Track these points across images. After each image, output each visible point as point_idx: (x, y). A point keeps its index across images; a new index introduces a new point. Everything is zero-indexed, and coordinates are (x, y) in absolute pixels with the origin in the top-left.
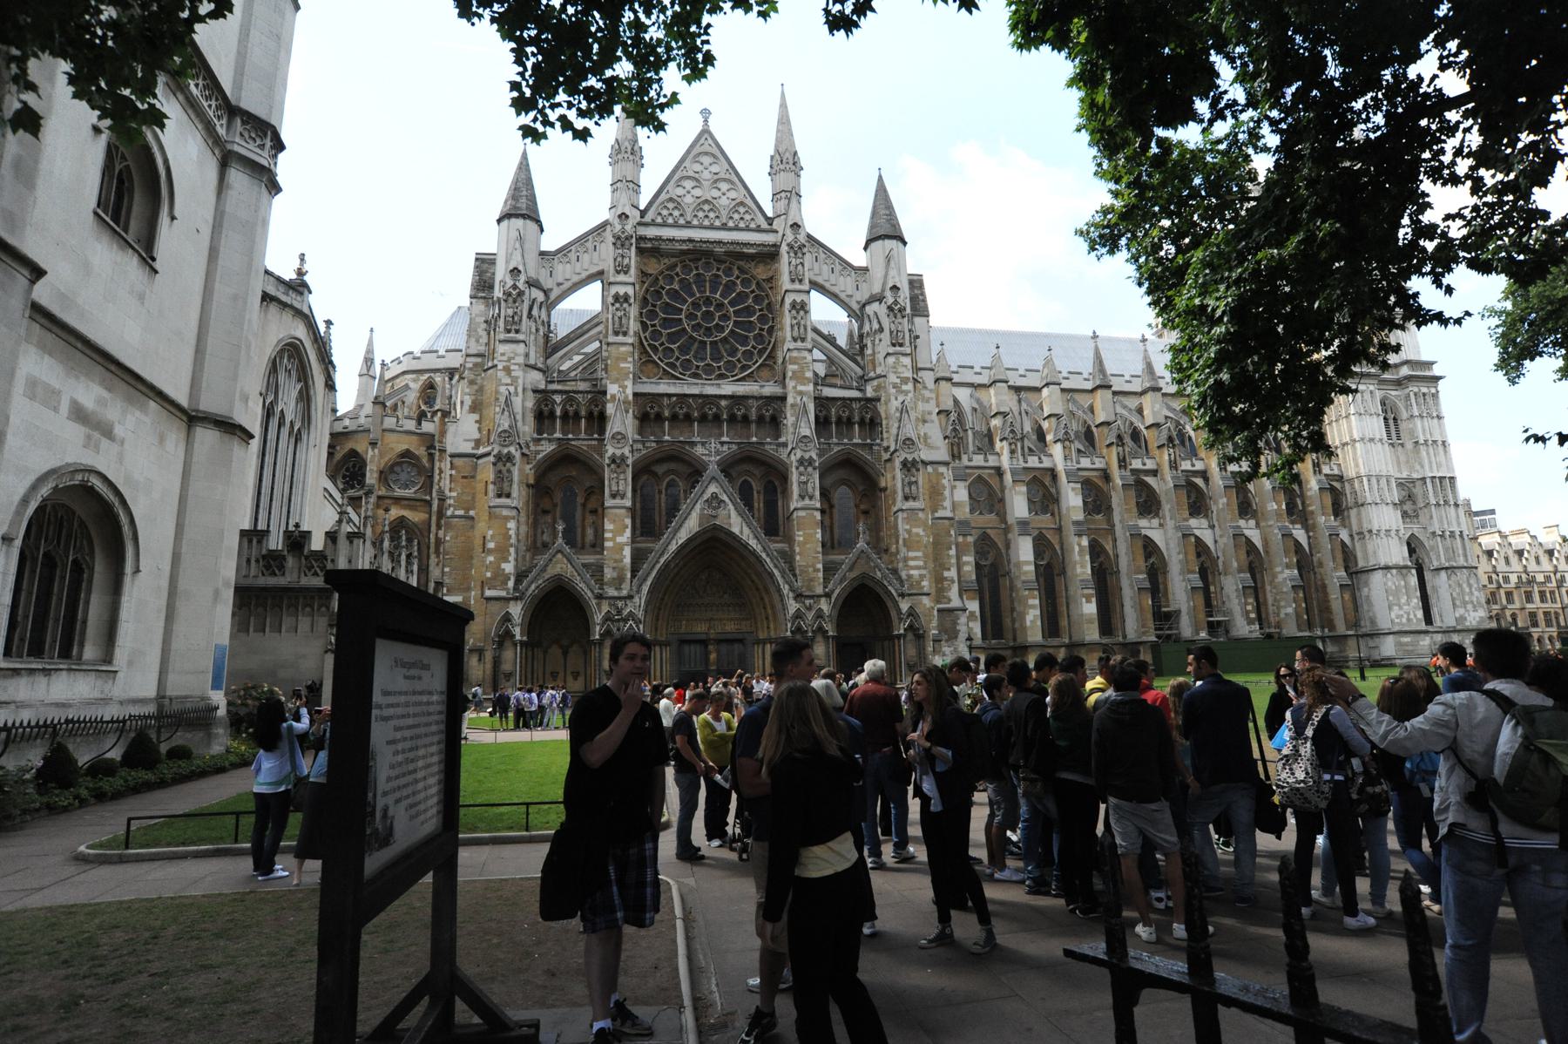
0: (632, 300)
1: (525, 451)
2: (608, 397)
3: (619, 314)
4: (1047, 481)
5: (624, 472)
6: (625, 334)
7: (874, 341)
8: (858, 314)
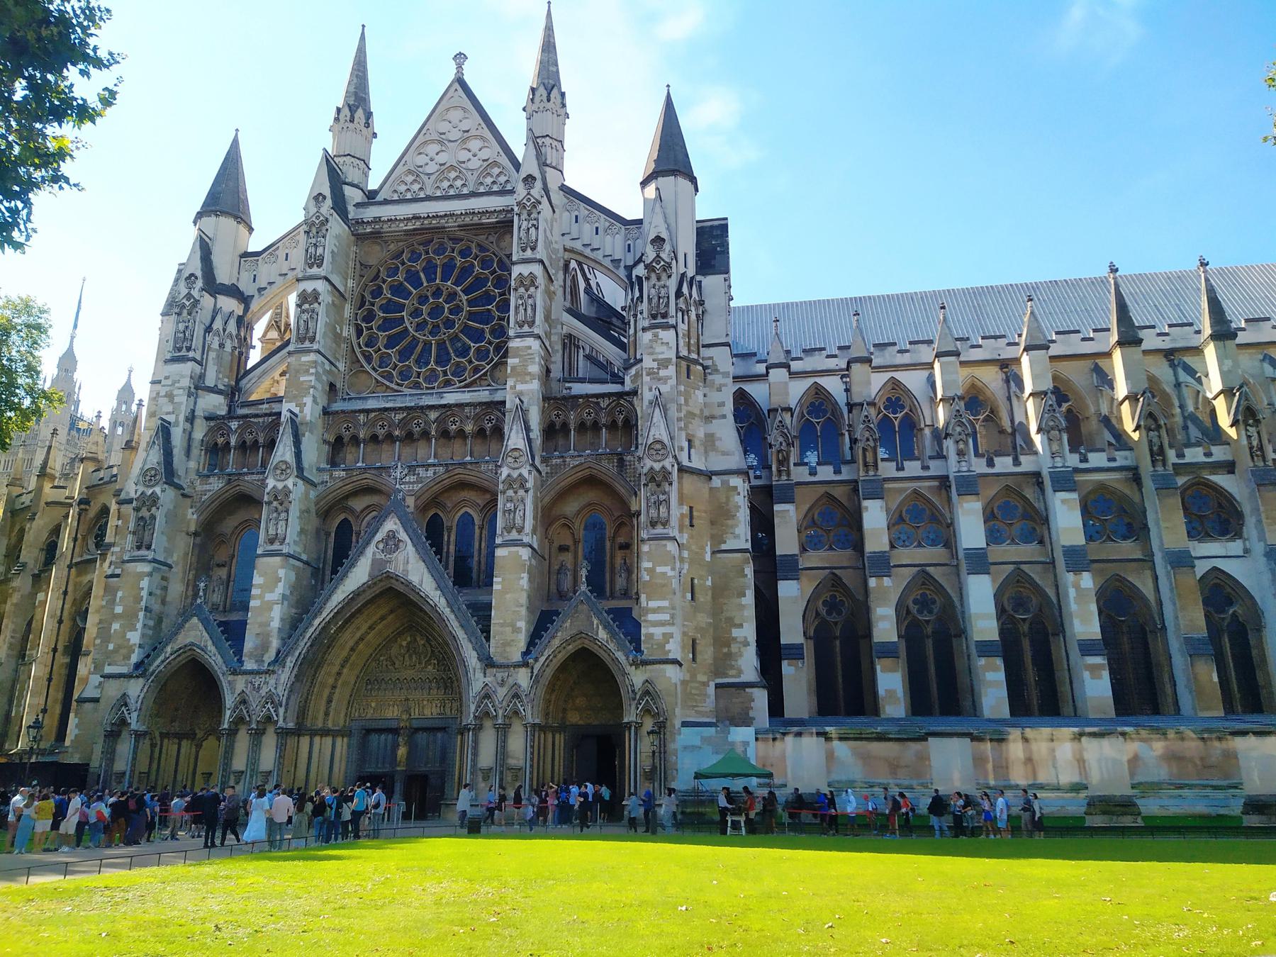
0: (326, 297)
2: (283, 419)
3: (305, 316)
4: (1030, 493)
5: (287, 511)
7: (635, 316)
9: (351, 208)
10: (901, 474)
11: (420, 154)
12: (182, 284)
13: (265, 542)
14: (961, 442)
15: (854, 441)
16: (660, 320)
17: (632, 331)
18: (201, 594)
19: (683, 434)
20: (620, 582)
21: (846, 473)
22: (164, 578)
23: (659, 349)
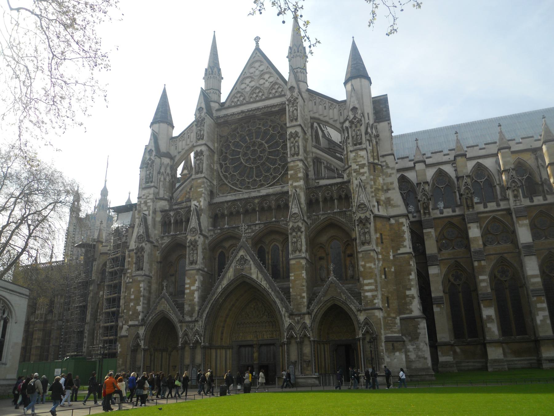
0: (206, 153)
1: (156, 244)
2: (192, 209)
3: (198, 162)
5: (197, 249)
6: (202, 172)
8: (341, 131)
9: (214, 112)
10: (486, 210)
11: (242, 83)
12: (147, 154)
13: (189, 264)
14: (515, 191)
15: (461, 195)
16: (358, 146)
17: (345, 152)
18: (165, 288)
19: (374, 199)
20: (350, 272)
21: (458, 212)
22: (149, 282)
23: (358, 160)
